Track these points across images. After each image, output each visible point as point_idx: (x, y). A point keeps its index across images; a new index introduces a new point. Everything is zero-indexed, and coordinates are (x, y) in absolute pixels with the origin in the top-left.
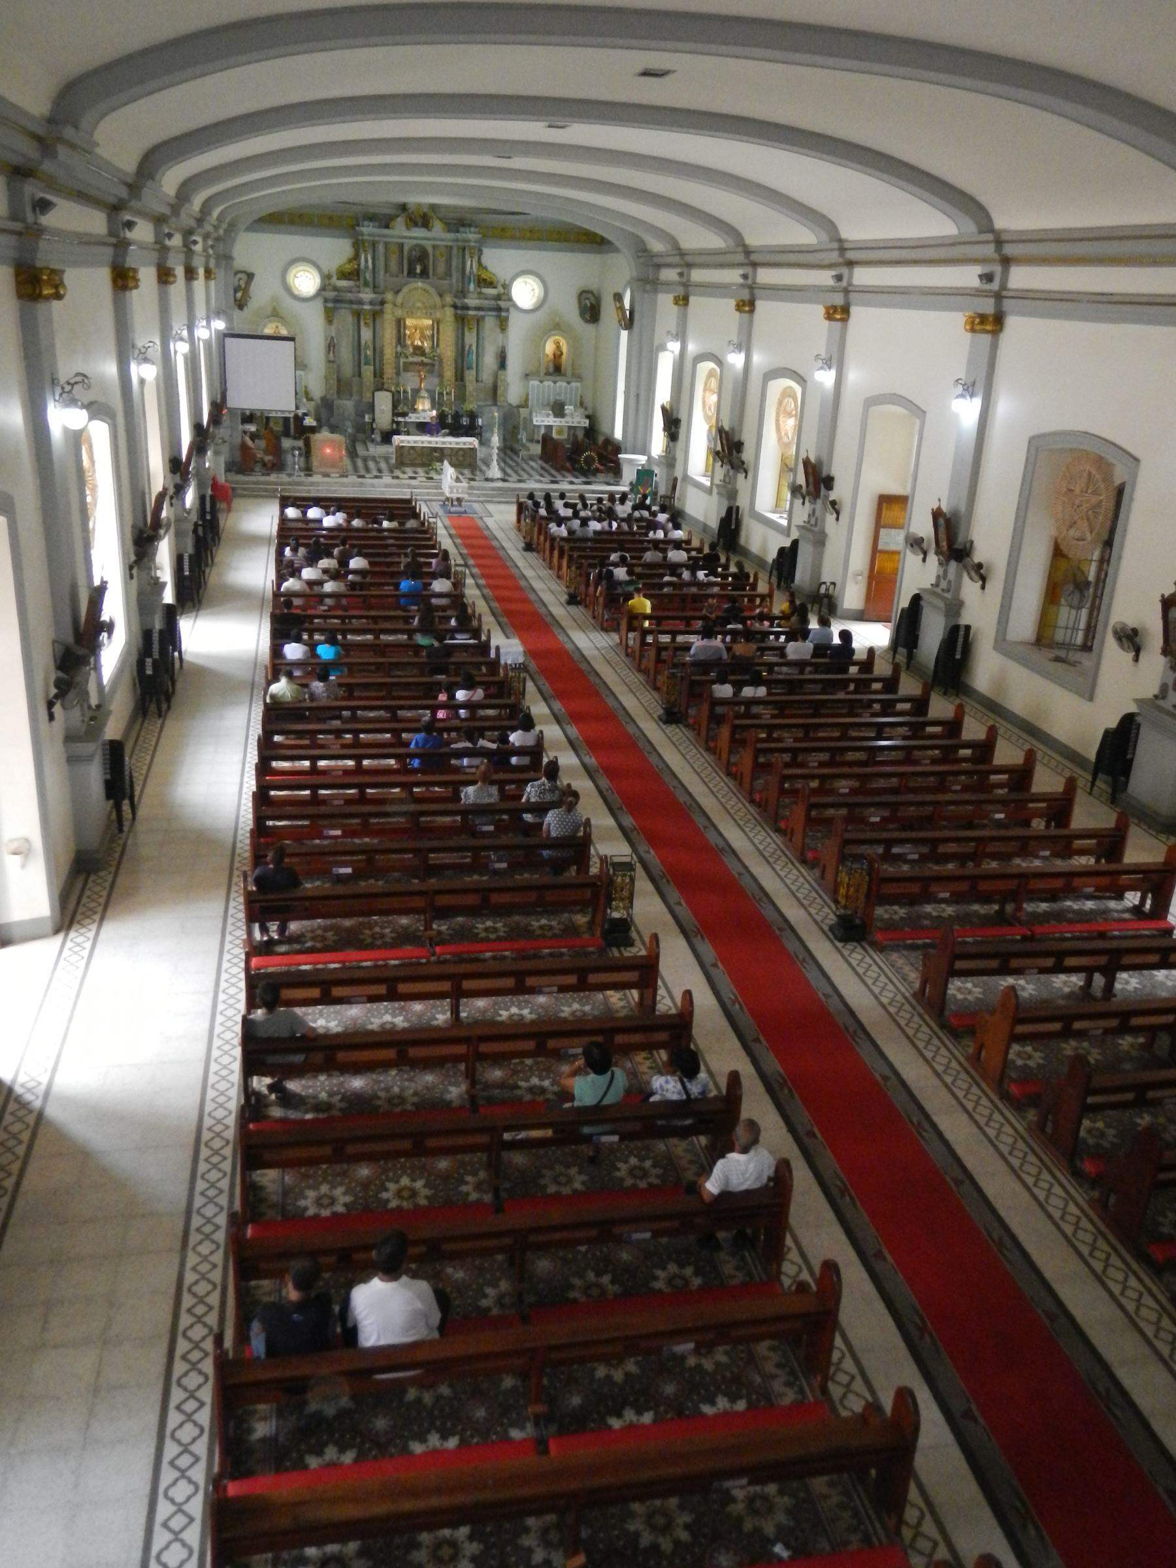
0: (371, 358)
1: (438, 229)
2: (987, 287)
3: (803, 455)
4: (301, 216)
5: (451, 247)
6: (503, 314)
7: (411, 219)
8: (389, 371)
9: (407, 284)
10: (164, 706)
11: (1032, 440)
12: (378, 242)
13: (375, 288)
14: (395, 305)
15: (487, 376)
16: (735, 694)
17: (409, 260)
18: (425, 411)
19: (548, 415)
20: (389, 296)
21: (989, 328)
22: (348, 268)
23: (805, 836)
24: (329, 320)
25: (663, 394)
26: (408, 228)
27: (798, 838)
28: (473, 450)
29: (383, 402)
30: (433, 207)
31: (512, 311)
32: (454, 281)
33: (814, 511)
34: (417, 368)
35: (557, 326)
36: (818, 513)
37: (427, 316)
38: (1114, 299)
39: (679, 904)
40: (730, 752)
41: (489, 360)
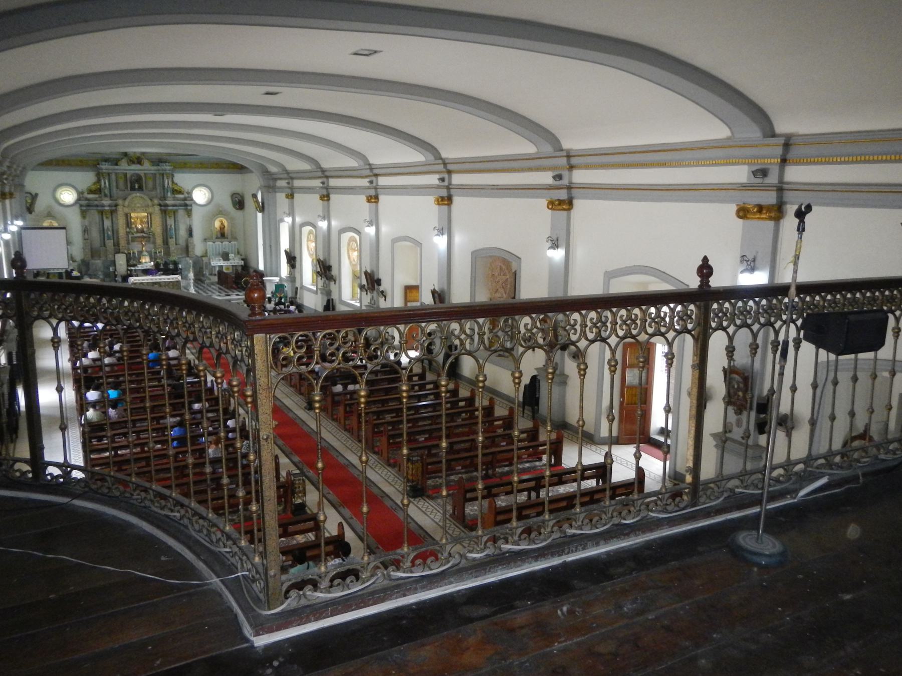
1: (147, 165)
2: (443, 184)
3: (364, 270)
4: (63, 161)
6: (189, 208)
7: (131, 160)
8: (123, 242)
9: (130, 194)
10: (14, 436)
11: (472, 253)
13: (111, 197)
14: (124, 206)
15: (182, 242)
16: (343, 390)
17: (131, 183)
18: (147, 262)
19: (220, 260)
21: (446, 202)
22: (94, 188)
23: (388, 453)
25: (285, 244)
27: (385, 454)
28: (178, 282)
29: (121, 261)
30: (143, 154)
31: (193, 205)
32: (158, 191)
33: (373, 297)
34: (140, 239)
35: (220, 212)
36: (375, 298)
38: (499, 187)
39: (329, 493)
40: (345, 419)
41: (183, 232)
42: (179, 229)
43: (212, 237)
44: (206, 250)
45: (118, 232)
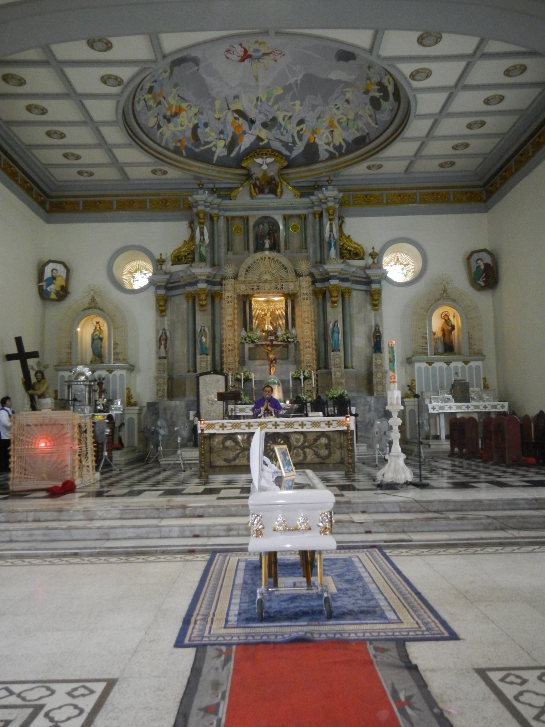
0: (208, 345)
5: (303, 218)
6: (374, 286)
7: (255, 186)
13: (213, 265)
20: (229, 271)
24: (162, 310)
26: (252, 198)
32: (311, 250)
37: (277, 290)
42: (352, 335)
43: (425, 352)
44: (414, 380)
45: (222, 340)
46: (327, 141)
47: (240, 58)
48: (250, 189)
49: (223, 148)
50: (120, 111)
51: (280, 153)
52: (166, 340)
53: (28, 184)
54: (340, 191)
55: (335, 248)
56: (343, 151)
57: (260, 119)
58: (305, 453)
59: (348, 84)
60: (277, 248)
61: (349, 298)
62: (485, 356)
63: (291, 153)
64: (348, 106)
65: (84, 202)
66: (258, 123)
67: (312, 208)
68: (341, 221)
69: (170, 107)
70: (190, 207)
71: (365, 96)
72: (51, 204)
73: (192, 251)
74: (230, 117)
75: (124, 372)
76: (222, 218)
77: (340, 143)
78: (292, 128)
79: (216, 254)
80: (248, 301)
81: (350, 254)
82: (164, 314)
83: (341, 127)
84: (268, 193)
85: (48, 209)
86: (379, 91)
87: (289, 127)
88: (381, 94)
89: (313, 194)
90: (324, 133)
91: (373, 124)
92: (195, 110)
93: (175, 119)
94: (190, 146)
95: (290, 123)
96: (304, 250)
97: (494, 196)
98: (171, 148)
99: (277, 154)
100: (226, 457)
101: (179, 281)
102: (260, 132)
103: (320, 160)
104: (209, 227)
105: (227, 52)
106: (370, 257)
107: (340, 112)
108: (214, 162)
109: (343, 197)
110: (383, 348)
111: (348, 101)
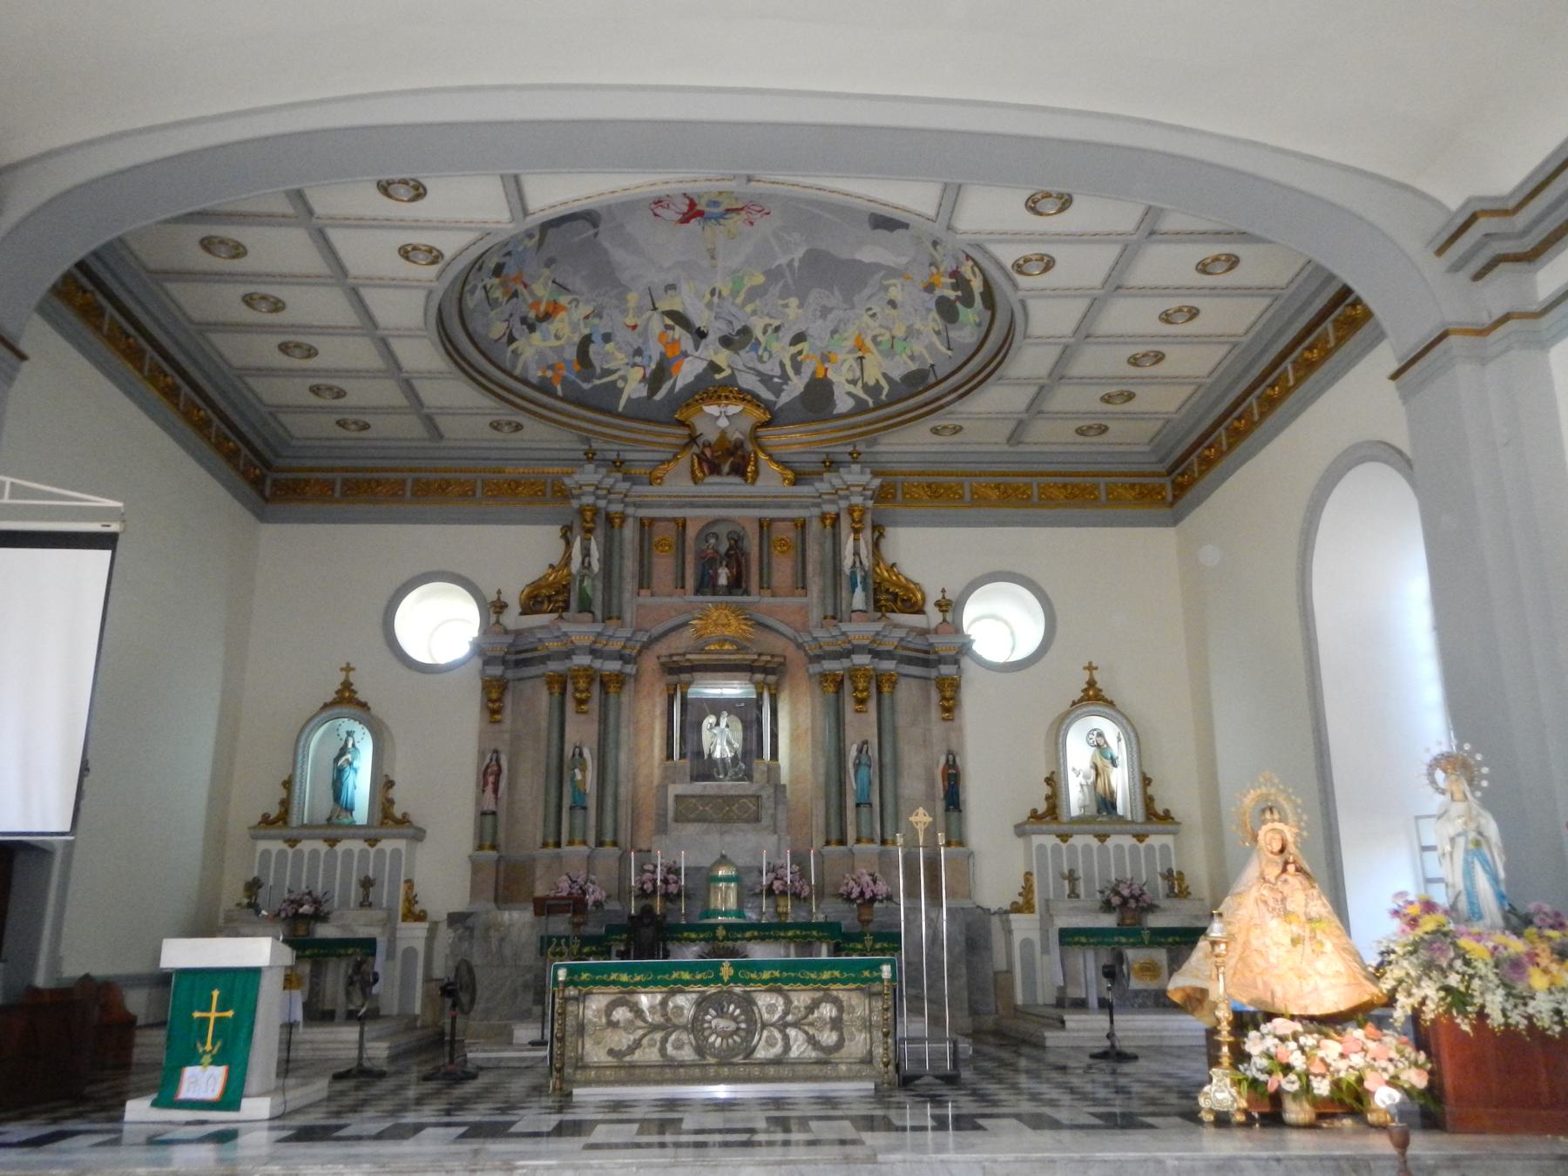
1: (771, 480)
5: (802, 525)
6: (946, 670)
12: (623, 518)
26: (696, 483)
46: (850, 377)
47: (680, 216)
48: (693, 465)
49: (640, 382)
50: (433, 312)
51: (756, 397)
52: (498, 774)
53: (231, 444)
54: (875, 474)
55: (864, 589)
56: (883, 397)
57: (716, 329)
58: (786, 1038)
59: (892, 272)
60: (744, 585)
61: (892, 693)
62: (1178, 824)
63: (778, 394)
64: (893, 312)
65: (345, 482)
66: (713, 337)
67: (818, 505)
68: (877, 534)
69: (536, 304)
70: (565, 495)
71: (926, 296)
72: (275, 483)
73: (564, 586)
74: (656, 324)
75: (401, 844)
76: (630, 521)
77: (877, 381)
78: (782, 350)
79: (615, 592)
80: (679, 695)
81: (895, 601)
82: (497, 717)
83: (880, 352)
84: (728, 474)
85: (267, 492)
86: (955, 287)
87: (775, 347)
88: (959, 293)
89: (822, 480)
90: (845, 361)
91: (943, 349)
92: (585, 309)
93: (544, 324)
94: (573, 377)
95: (778, 339)
96: (800, 591)
97: (1189, 496)
98: (534, 381)
99: (749, 397)
100: (613, 1046)
101: (535, 649)
102: (716, 353)
103: (835, 412)
104: (601, 539)
105: (656, 203)
106: (937, 609)
107: (877, 324)
108: (620, 409)
109: (881, 486)
110: (964, 801)
111: (892, 304)
